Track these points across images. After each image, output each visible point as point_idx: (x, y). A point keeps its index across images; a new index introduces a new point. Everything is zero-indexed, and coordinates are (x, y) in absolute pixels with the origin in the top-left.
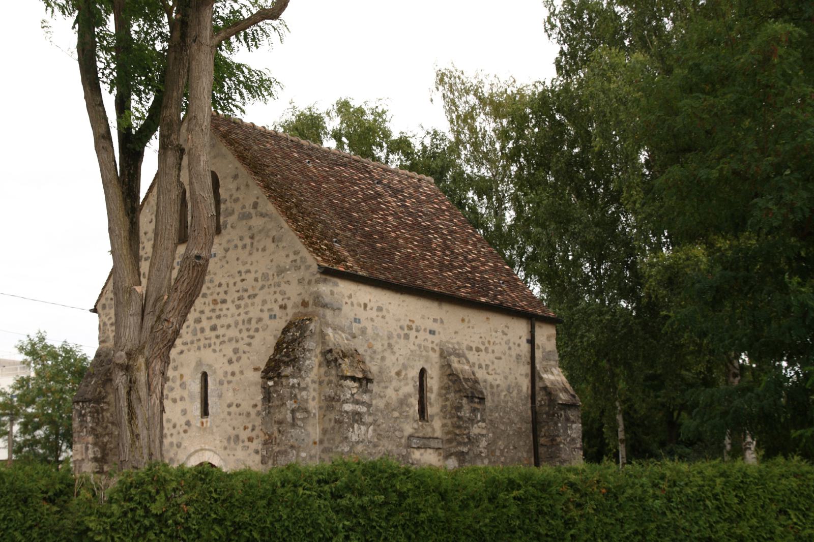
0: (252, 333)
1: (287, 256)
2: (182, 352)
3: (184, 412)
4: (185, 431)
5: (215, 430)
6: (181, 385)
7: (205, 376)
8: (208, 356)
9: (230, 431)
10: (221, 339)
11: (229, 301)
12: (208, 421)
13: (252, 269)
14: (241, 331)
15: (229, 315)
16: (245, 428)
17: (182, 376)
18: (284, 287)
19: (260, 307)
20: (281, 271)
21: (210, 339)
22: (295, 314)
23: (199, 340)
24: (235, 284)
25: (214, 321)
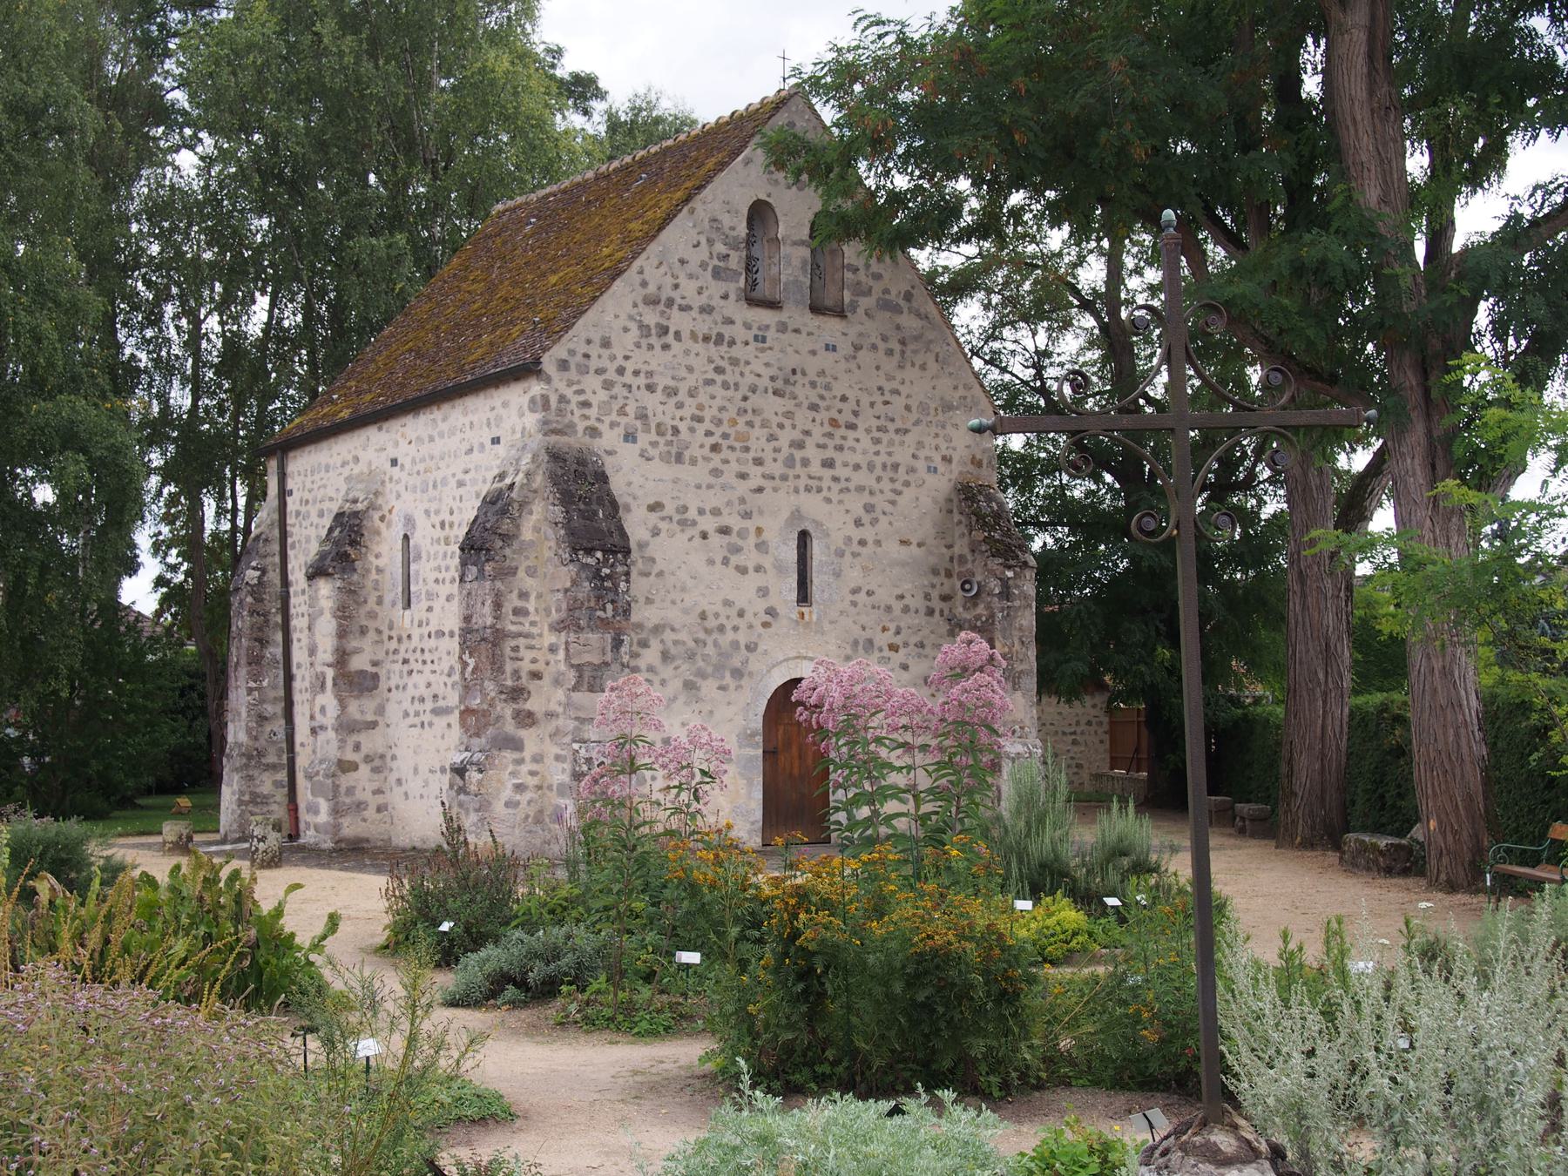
0: (898, 486)
1: (956, 388)
2: (760, 490)
3: (763, 592)
4: (766, 625)
5: (827, 627)
6: (757, 546)
7: (804, 536)
8: (813, 506)
9: (857, 631)
10: (843, 484)
11: (861, 427)
12: (812, 613)
13: (904, 390)
14: (879, 479)
15: (859, 451)
16: (884, 629)
17: (759, 531)
18: (950, 430)
19: (912, 450)
20: (948, 407)
21: (820, 479)
22: (961, 473)
23: (798, 477)
24: (872, 404)
25: (830, 453)
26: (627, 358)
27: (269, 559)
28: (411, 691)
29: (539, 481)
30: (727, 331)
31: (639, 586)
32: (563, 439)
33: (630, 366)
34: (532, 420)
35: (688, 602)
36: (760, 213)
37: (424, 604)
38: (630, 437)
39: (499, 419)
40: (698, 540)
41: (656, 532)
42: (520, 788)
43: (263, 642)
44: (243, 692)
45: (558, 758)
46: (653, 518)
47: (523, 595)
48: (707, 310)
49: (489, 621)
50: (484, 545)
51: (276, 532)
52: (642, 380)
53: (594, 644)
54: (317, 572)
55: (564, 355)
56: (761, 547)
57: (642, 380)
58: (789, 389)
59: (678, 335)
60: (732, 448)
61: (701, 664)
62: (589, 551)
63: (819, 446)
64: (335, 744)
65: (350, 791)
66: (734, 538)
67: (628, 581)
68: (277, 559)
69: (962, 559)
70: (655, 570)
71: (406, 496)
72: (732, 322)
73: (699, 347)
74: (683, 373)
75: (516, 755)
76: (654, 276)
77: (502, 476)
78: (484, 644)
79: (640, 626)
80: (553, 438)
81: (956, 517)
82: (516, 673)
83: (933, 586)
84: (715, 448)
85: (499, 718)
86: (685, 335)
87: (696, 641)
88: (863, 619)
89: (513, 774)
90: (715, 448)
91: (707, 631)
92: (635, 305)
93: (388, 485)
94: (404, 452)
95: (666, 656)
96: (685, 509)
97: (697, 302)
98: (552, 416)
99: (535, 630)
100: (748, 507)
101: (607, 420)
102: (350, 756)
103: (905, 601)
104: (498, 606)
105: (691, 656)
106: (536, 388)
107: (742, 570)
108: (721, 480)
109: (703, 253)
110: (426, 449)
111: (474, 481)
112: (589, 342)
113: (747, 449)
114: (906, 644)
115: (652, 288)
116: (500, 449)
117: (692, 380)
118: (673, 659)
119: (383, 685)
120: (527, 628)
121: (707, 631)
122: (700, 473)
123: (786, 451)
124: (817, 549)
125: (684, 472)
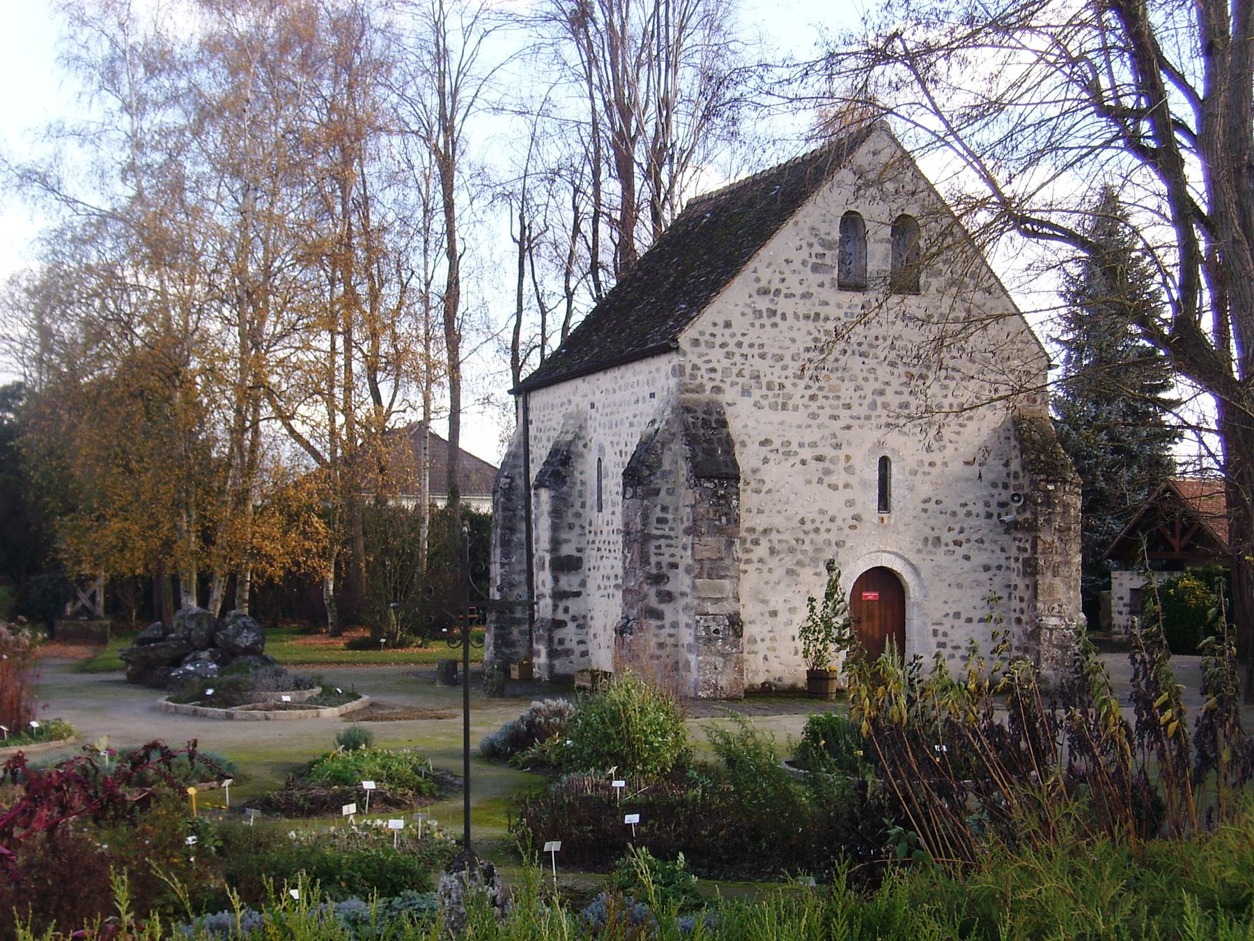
2: (849, 427)
3: (850, 503)
7: (884, 463)
9: (927, 531)
16: (950, 529)
17: (848, 458)
26: (743, 335)
27: (517, 470)
28: (602, 572)
29: (676, 428)
30: (824, 311)
31: (747, 499)
32: (696, 396)
33: (746, 341)
34: (673, 382)
35: (791, 512)
36: (851, 222)
37: (610, 510)
38: (746, 392)
39: (654, 380)
40: (799, 466)
41: (766, 461)
42: (661, 645)
43: (512, 530)
44: (498, 566)
45: (688, 625)
46: (764, 451)
47: (664, 509)
48: (805, 296)
49: (640, 527)
50: (640, 473)
51: (522, 450)
52: (756, 351)
53: (711, 544)
54: (540, 484)
55: (697, 336)
56: (849, 470)
57: (756, 351)
58: (872, 351)
59: (784, 317)
60: (826, 397)
61: (800, 556)
62: (709, 479)
63: (896, 393)
64: (550, 609)
65: (561, 642)
66: (827, 464)
67: (738, 499)
68: (522, 470)
69: (1016, 476)
70: (765, 489)
71: (600, 431)
72: (827, 304)
73: (802, 322)
74: (788, 343)
75: (659, 623)
76: (765, 274)
77: (653, 422)
78: (637, 540)
79: (751, 530)
80: (688, 396)
81: (1013, 442)
82: (659, 564)
83: (992, 496)
84: (812, 398)
85: (646, 596)
86: (790, 316)
87: (797, 541)
88: (932, 522)
89: (656, 635)
90: (812, 398)
91: (806, 533)
92: (750, 296)
93: (589, 422)
94: (598, 398)
95: (772, 551)
96: (789, 443)
97: (799, 290)
98: (687, 379)
99: (672, 534)
100: (838, 441)
101: (728, 381)
102: (560, 616)
103: (968, 508)
104: (645, 517)
105: (791, 550)
106: (675, 359)
107: (834, 487)
108: (817, 421)
109: (804, 254)
110: (611, 398)
111: (640, 423)
112: (715, 325)
113: (838, 397)
114: (968, 541)
115: (763, 283)
116: (655, 401)
117: (794, 349)
118: (778, 553)
119: (586, 565)
120: (667, 532)
121: (806, 533)
122: (801, 416)
123: (869, 399)
124: (895, 470)
125: (787, 416)
